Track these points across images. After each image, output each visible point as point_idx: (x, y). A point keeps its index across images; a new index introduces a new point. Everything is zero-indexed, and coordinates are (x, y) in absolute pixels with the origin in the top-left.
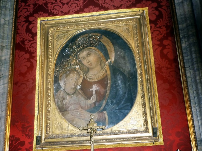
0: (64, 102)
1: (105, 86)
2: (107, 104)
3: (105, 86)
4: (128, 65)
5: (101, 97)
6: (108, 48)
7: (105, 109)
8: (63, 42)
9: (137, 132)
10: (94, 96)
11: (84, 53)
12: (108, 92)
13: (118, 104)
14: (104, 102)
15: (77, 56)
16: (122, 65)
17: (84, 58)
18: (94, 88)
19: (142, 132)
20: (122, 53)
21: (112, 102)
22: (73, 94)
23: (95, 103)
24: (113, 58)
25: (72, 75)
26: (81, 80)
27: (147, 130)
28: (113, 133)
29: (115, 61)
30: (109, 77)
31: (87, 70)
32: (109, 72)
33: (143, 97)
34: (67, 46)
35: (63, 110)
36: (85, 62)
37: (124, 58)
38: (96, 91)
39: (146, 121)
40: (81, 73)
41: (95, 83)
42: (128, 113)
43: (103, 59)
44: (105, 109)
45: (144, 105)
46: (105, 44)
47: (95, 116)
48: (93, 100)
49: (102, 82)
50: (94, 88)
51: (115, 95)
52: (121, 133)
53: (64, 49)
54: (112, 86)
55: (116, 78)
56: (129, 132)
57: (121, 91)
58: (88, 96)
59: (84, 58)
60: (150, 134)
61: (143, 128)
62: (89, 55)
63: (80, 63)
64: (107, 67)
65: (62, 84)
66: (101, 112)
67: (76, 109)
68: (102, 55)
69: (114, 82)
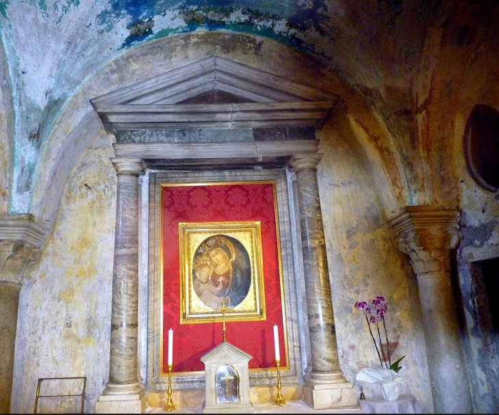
0: (200, 288)
1: (228, 278)
2: (230, 291)
3: (228, 278)
4: (245, 264)
5: (225, 286)
6: (231, 249)
7: (228, 294)
8: (198, 245)
9: (250, 311)
10: (221, 285)
11: (213, 252)
12: (230, 283)
13: (237, 291)
14: (228, 289)
15: (208, 255)
16: (240, 263)
17: (213, 256)
18: (221, 279)
19: (254, 312)
20: (241, 254)
21: (233, 290)
22: (206, 283)
23: (221, 290)
24: (234, 258)
25: (204, 268)
26: (211, 273)
27: (256, 310)
28: (234, 312)
29: (236, 259)
30: (231, 271)
31: (216, 266)
32: (231, 268)
33: (255, 288)
34: (201, 245)
35: (199, 294)
36: (214, 259)
37: (242, 258)
38: (222, 281)
39: (256, 304)
40: (212, 267)
41: (221, 275)
42: (244, 298)
43: (228, 259)
44: (228, 294)
45: (255, 293)
46: (228, 246)
47: (221, 299)
48: (220, 288)
49: (226, 275)
50: (221, 279)
51: (235, 285)
52: (239, 312)
53: (199, 248)
54: (233, 278)
55: (236, 272)
56: (245, 311)
57: (239, 281)
58: (217, 285)
59: (213, 256)
60: (258, 312)
61: (254, 308)
62: (217, 253)
63: (211, 260)
64: (230, 264)
65: (197, 275)
66: (226, 296)
67: (208, 294)
68: (226, 254)
69: (235, 275)
